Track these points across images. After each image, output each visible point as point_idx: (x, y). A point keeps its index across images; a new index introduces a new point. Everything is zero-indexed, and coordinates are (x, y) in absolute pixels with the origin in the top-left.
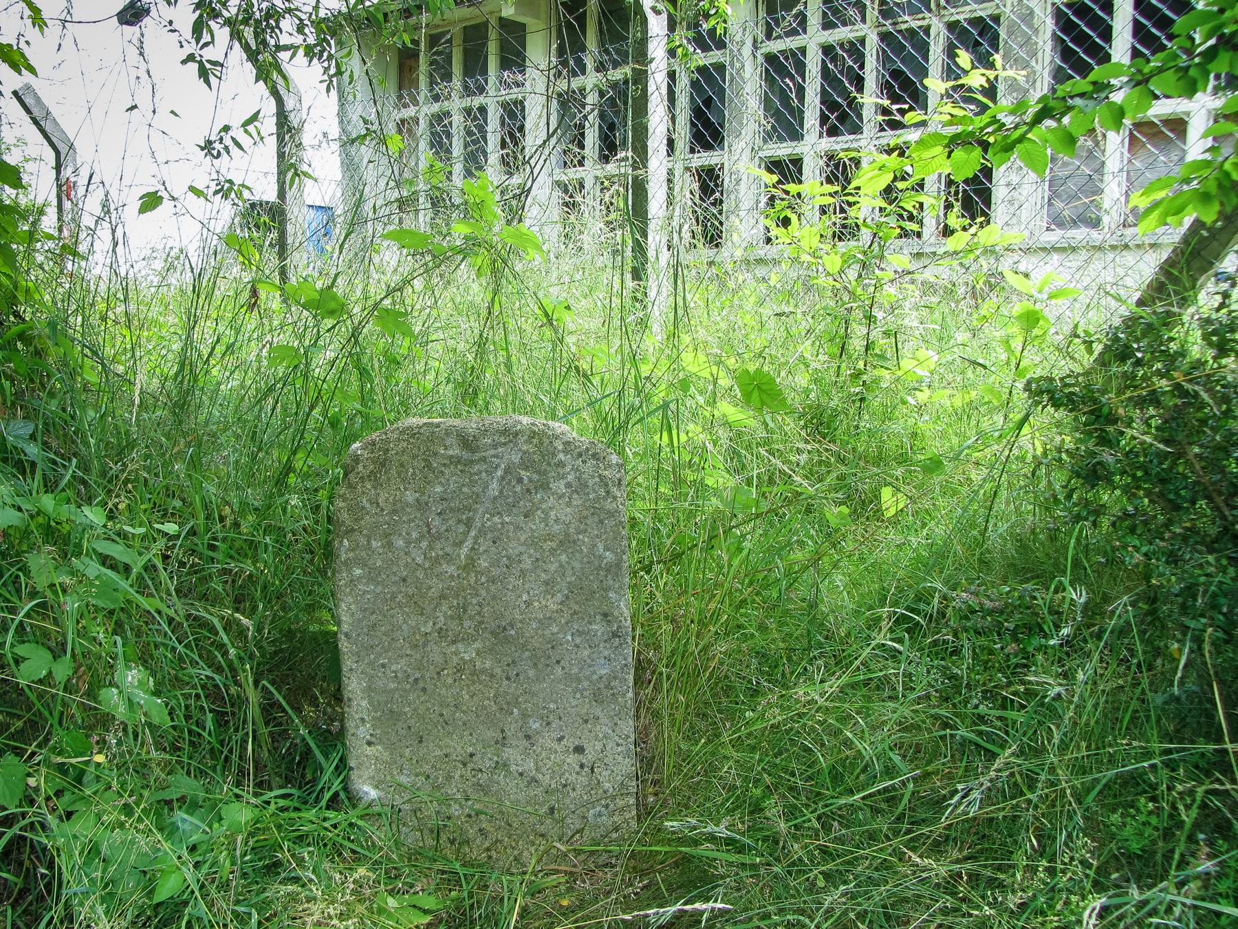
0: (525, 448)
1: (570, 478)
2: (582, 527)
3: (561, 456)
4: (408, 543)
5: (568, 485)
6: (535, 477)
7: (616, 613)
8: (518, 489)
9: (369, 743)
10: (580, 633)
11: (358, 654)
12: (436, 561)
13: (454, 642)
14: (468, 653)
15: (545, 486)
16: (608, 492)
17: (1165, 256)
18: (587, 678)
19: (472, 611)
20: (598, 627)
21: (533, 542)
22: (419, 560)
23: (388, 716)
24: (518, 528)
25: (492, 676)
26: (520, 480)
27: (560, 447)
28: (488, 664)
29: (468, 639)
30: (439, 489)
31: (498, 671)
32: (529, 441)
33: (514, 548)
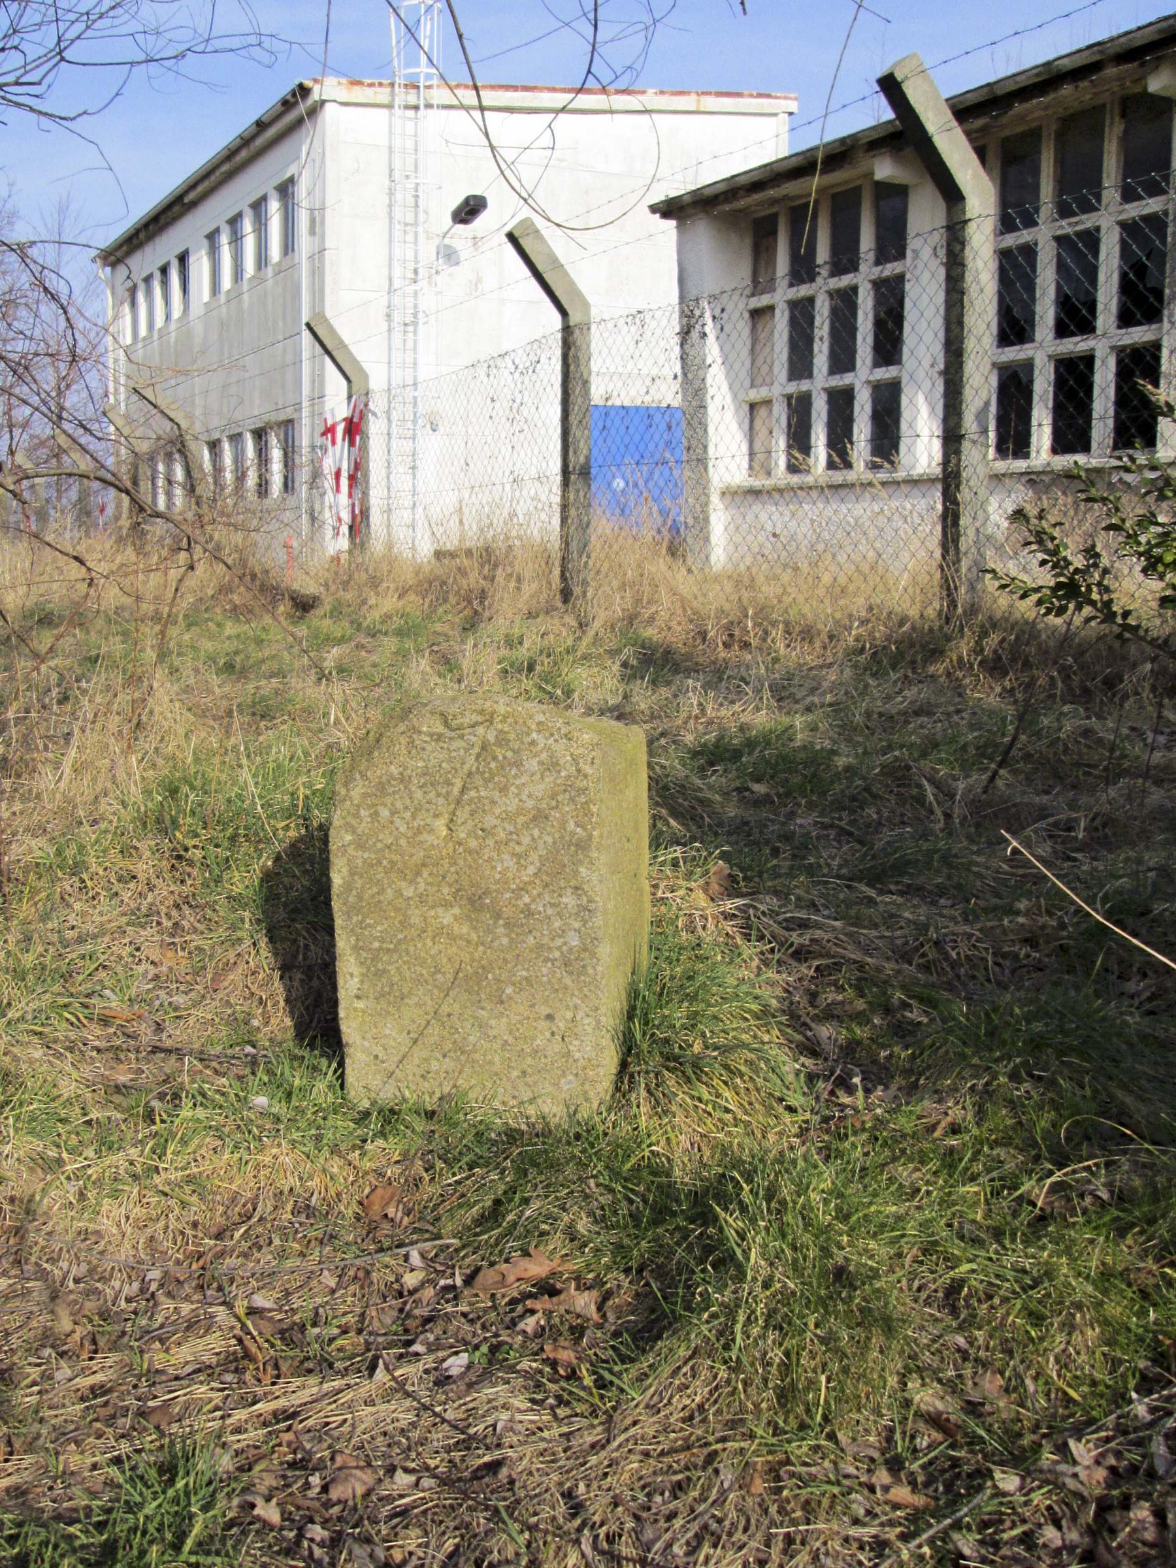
0: (500, 726)
1: (544, 755)
2: (554, 803)
3: (534, 735)
4: (393, 814)
5: (541, 763)
6: (509, 754)
7: (586, 887)
8: (493, 765)
9: (358, 997)
10: (553, 905)
11: (348, 913)
12: (419, 831)
13: (433, 907)
14: (446, 917)
15: (518, 764)
16: (579, 771)
17: (732, 408)
18: (559, 948)
19: (450, 878)
20: (569, 900)
21: (509, 817)
22: (403, 829)
23: (373, 972)
24: (493, 802)
25: (468, 942)
26: (495, 758)
27: (534, 727)
28: (465, 930)
29: (447, 905)
30: (421, 764)
31: (474, 937)
32: (503, 721)
33: (489, 821)
